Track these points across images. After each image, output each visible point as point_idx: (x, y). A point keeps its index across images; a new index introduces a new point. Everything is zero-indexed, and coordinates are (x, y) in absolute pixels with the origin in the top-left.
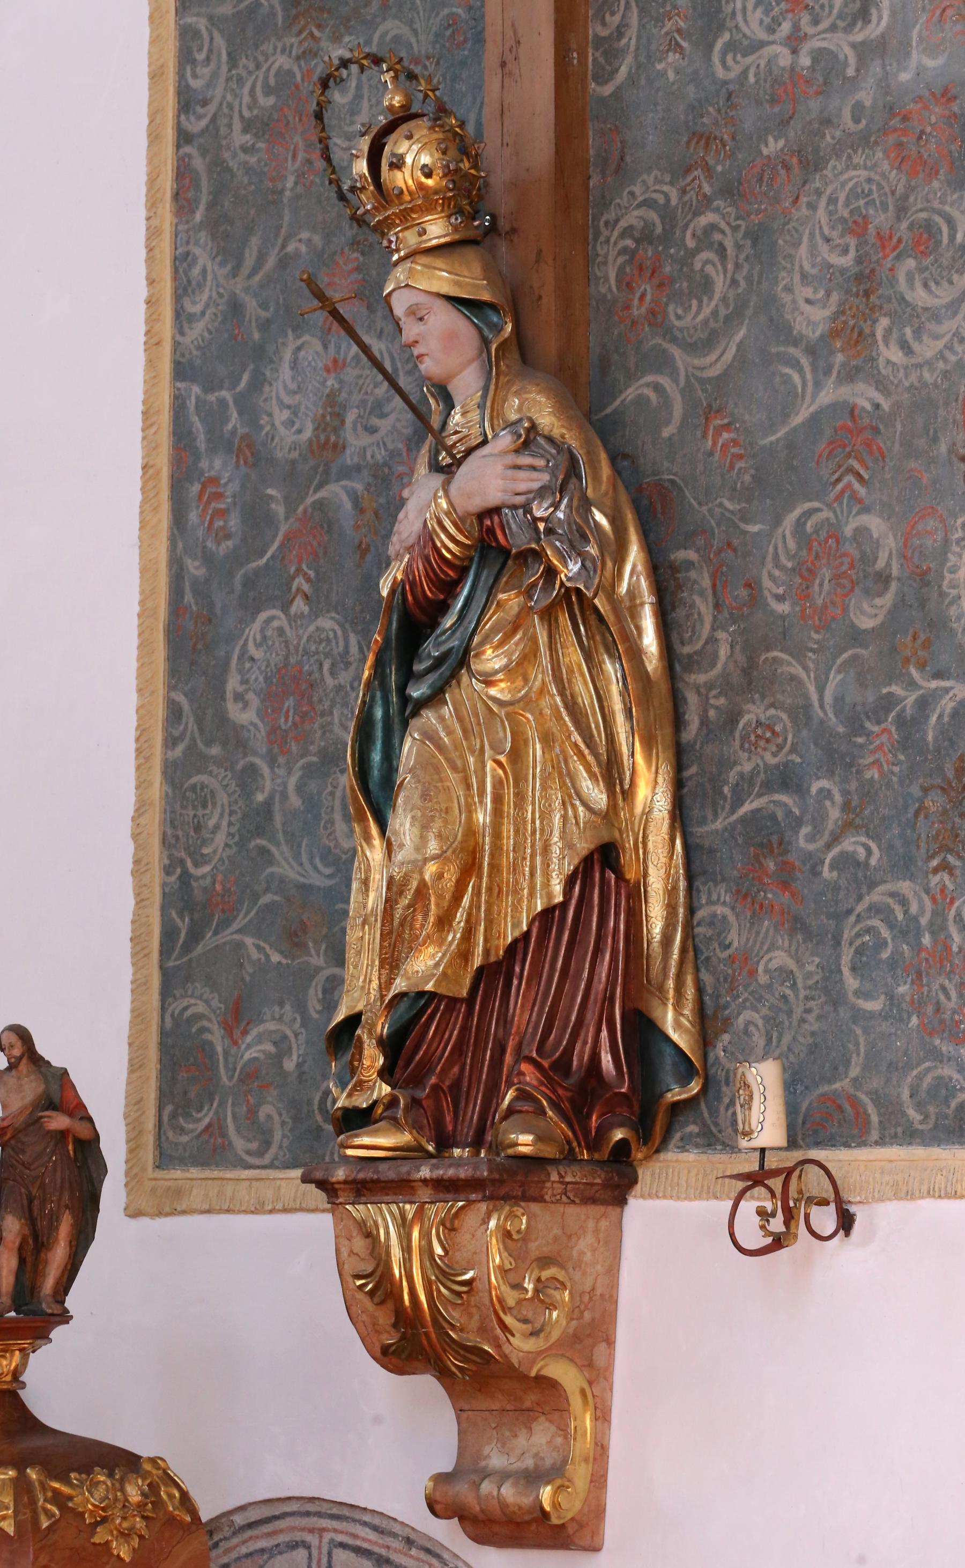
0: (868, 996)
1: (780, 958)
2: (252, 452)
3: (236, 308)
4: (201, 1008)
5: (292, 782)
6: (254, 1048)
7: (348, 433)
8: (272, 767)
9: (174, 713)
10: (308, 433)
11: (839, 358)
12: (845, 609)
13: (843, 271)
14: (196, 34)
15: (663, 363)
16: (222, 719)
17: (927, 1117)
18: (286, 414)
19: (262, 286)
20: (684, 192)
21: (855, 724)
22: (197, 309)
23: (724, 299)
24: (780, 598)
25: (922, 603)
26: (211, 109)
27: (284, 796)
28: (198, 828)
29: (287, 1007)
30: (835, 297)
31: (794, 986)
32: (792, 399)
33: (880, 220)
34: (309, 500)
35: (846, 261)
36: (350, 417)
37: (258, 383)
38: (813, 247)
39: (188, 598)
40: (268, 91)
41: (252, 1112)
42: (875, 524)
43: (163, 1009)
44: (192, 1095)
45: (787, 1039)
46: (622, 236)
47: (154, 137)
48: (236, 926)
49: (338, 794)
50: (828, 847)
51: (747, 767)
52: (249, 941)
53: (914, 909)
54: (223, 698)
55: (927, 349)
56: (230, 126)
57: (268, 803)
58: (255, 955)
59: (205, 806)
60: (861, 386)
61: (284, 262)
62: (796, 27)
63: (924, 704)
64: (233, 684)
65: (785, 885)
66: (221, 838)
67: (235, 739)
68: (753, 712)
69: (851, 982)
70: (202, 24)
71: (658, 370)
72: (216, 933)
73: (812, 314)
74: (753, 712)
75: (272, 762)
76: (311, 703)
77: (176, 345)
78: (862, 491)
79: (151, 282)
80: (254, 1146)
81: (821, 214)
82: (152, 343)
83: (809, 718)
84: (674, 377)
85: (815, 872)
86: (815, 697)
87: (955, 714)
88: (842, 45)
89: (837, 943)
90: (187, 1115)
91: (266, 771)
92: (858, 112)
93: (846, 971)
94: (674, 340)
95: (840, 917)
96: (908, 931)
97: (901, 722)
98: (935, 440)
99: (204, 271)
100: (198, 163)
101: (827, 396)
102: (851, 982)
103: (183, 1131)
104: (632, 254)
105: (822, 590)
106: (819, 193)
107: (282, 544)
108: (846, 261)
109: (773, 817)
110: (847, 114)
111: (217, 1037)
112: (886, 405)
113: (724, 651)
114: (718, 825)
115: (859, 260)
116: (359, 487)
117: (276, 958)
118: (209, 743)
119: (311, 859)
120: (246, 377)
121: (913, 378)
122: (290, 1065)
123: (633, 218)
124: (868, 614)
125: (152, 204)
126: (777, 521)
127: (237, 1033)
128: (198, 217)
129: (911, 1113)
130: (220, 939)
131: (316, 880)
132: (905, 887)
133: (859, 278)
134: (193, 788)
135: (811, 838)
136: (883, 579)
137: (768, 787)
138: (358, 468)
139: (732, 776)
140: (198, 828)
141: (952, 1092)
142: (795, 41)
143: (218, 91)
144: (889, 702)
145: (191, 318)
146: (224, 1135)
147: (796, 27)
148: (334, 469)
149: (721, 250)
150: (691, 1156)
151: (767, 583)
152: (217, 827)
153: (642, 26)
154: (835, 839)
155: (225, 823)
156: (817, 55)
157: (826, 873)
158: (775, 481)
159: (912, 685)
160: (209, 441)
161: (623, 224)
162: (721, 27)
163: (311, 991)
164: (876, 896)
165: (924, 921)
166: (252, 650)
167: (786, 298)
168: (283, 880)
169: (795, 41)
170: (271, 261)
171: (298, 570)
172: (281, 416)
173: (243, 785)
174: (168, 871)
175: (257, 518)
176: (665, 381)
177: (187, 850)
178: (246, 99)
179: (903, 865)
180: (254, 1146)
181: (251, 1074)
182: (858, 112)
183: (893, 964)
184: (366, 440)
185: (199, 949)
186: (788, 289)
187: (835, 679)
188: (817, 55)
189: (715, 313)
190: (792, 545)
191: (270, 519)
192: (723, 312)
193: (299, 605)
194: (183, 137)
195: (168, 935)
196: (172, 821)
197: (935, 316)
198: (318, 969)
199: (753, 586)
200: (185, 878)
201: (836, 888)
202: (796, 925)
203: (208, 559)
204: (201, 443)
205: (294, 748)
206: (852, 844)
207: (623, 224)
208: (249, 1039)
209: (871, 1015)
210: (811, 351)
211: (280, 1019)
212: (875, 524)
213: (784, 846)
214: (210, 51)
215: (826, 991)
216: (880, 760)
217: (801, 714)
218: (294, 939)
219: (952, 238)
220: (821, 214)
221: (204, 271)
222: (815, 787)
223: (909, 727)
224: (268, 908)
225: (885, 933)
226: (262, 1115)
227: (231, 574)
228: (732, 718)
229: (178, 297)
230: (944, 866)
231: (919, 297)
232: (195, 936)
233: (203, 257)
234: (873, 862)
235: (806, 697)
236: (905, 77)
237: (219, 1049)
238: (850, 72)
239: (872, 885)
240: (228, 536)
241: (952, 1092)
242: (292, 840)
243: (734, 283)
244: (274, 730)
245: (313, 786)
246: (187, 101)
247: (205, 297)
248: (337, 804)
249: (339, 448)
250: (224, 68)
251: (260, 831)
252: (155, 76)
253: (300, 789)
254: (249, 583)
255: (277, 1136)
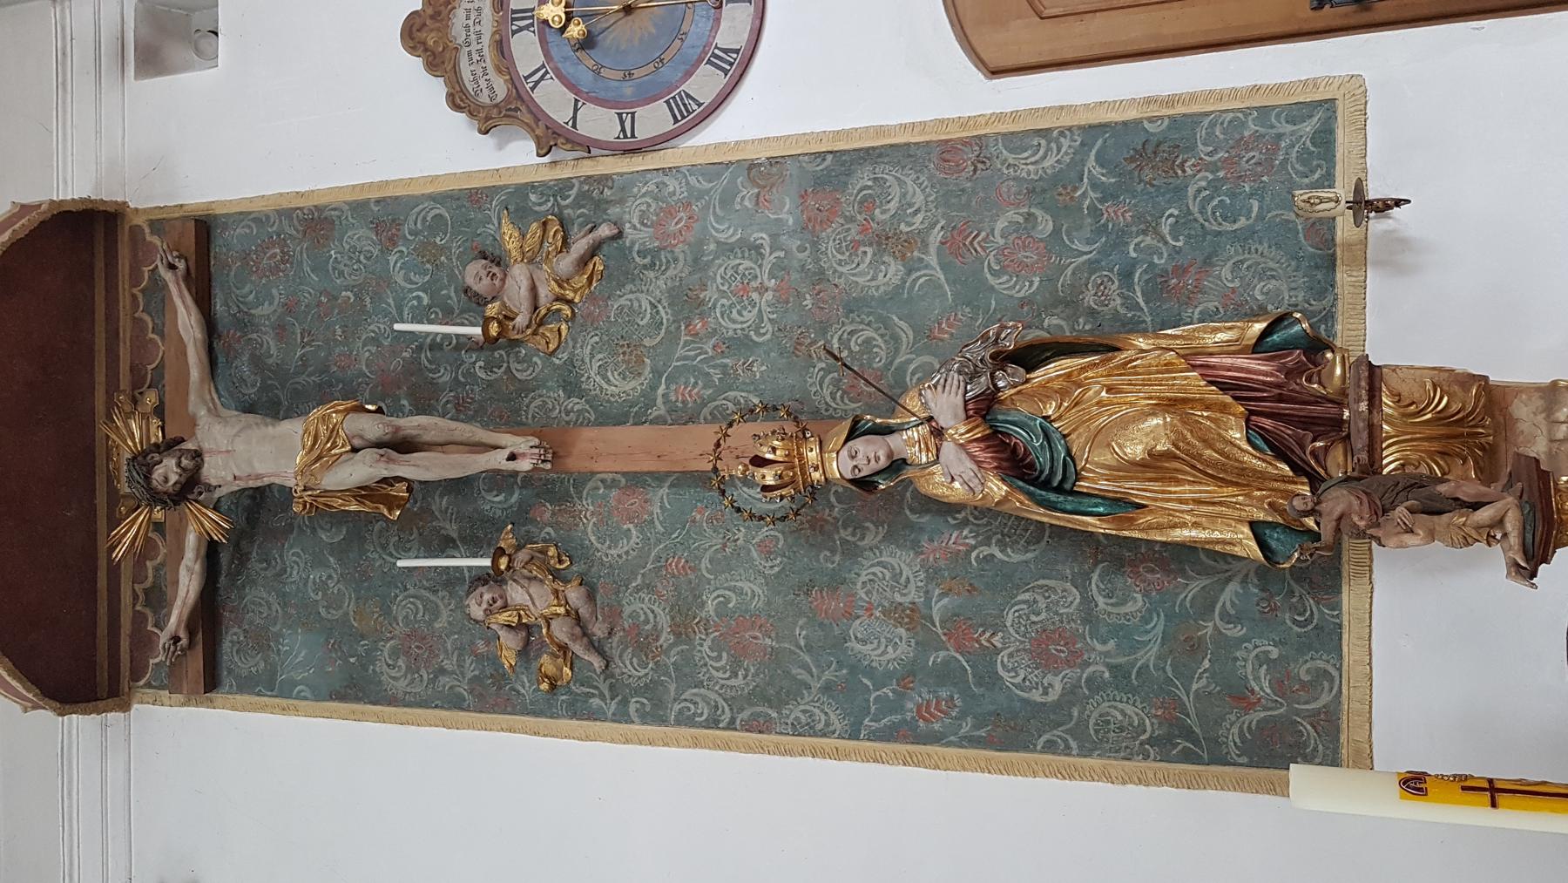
0: (1250, 211)
1: (1226, 272)
2: (908, 675)
3: (827, 688)
4: (1235, 730)
5: (1099, 647)
6: (1262, 685)
7: (906, 600)
8: (1089, 664)
9: (1050, 747)
10: (902, 631)
11: (916, 253)
12: (1041, 240)
13: (874, 255)
14: (681, 712)
15: (902, 369)
16: (1057, 705)
17: (1319, 166)
18: (890, 649)
19: (818, 667)
20: (820, 359)
21: (1101, 230)
22: (823, 718)
23: (876, 330)
24: (1031, 283)
25: (1044, 191)
26: (721, 702)
27: (1107, 654)
28: (1122, 729)
29: (1238, 654)
30: (886, 259)
31: (1242, 262)
32: (932, 283)
33: (854, 233)
34: (940, 631)
35: (869, 251)
36: (898, 598)
37: (870, 671)
38: (861, 274)
39: (982, 733)
40: (719, 658)
41: (1304, 686)
42: (1000, 225)
43: (1235, 764)
44: (1290, 739)
45: (1271, 264)
46: (834, 399)
47: (726, 746)
48: (1185, 698)
49: (1109, 609)
50: (1166, 243)
51: (1119, 301)
52: (1195, 687)
53: (1204, 184)
54: (1044, 704)
55: (919, 199)
56: (732, 687)
57: (1112, 668)
58: (1204, 682)
59: (1108, 722)
60: (931, 239)
61: (809, 649)
62: (756, 289)
63: (1095, 185)
64: (1036, 696)
65: (1186, 271)
66: (1129, 710)
67: (1070, 693)
68: (1089, 300)
69: (1242, 222)
70: (677, 707)
71: (905, 372)
72: (1188, 716)
73: (893, 271)
74: (1089, 300)
75: (1087, 664)
76: (1054, 632)
77: (840, 737)
78: (983, 234)
79: (803, 753)
80: (1326, 684)
81: (844, 269)
82: (837, 755)
83: (1098, 261)
84: (909, 362)
85: (1178, 251)
86: (1086, 257)
87: (1102, 166)
88: (770, 259)
89: (1219, 233)
90: (1306, 745)
91: (1091, 669)
92: (802, 249)
93: (1236, 227)
94: (891, 363)
95: (1205, 232)
96: (1215, 186)
97: (1102, 200)
98: (963, 190)
99: (804, 712)
100: (745, 715)
101: (932, 259)
102: (1242, 222)
103: (1315, 749)
104: (844, 392)
105: (1030, 256)
106: (835, 271)
107: (962, 654)
108: (869, 251)
109: (1147, 282)
110: (801, 256)
111: (1257, 716)
112: (943, 222)
113: (1055, 321)
114: (1148, 319)
115: (871, 245)
116: (937, 592)
117: (1206, 664)
118: (1071, 716)
119: (1147, 632)
120: (865, 681)
121: (931, 206)
122: (1275, 653)
123: (826, 393)
124: (1045, 225)
125: (762, 749)
126: (992, 288)
127: (1253, 699)
128: (774, 715)
129: (1317, 176)
130: (1192, 712)
131: (1160, 628)
132: (1191, 191)
133: (879, 244)
134: (1096, 732)
135: (1160, 255)
136: (1029, 217)
137: (1130, 287)
138: (927, 592)
139: (1122, 311)
140: (1122, 729)
141: (1305, 149)
142: (762, 290)
143: (713, 696)
144: (1093, 210)
145: (827, 724)
146: (1318, 712)
147: (756, 289)
148: (924, 611)
149: (852, 333)
150: (1339, 327)
151: (1021, 294)
152: (1123, 712)
153: (737, 389)
154: (1163, 239)
155: (1120, 705)
156: (772, 276)
157: (1180, 244)
158: (972, 290)
159: (1084, 195)
160: (897, 713)
161: (828, 399)
162: (747, 336)
163: (1229, 633)
164: (1195, 210)
165: (1211, 177)
166: (1018, 680)
167: (882, 289)
168: (1159, 658)
169: (762, 290)
170: (808, 659)
171: (978, 641)
172: (891, 653)
173: (1099, 689)
174: (1146, 757)
175: (946, 674)
176: (912, 367)
177: (1135, 739)
178: (720, 675)
179: (1179, 192)
180: (1326, 684)
181: (1279, 686)
182: (802, 249)
183: (1233, 196)
184: (912, 587)
185: (1197, 730)
186: (878, 288)
187: (1077, 246)
188: (772, 276)
189: (882, 336)
190: (1005, 278)
191: (946, 662)
192: (882, 331)
193: (997, 641)
194: (731, 726)
195: (1188, 757)
196: (1116, 752)
197: (904, 195)
198: (1216, 627)
199: (1023, 302)
200: (1152, 741)
201: (1189, 236)
202: (1208, 262)
203: (963, 715)
204: (896, 718)
205: (1079, 645)
206: (1165, 230)
207: (828, 399)
208: (1257, 689)
209: (1260, 208)
210: (909, 273)
211: (1245, 660)
212: (1000, 225)
213: (1164, 273)
214: (691, 701)
215: (1246, 239)
216: (1119, 214)
217: (1093, 267)
218: (1195, 648)
219: (869, 187)
220: (844, 269)
221: (804, 712)
222: (1133, 255)
223: (1108, 195)
224: (1175, 668)
225: (1215, 202)
226: (1306, 678)
227: (973, 696)
228: (1092, 313)
229: (815, 735)
230: (1182, 166)
231: (893, 206)
232: (1189, 734)
233: (795, 712)
234: (1176, 213)
235: (1084, 263)
236: (791, 222)
237: (1262, 715)
238: (782, 254)
239: (1189, 213)
240: (952, 698)
241: (1305, 149)
242: (1135, 647)
243: (869, 324)
244: (1068, 663)
245: (1103, 630)
246: (713, 723)
247: (817, 711)
248: (1115, 610)
249: (914, 607)
250: (702, 691)
251: (1127, 676)
252: (696, 743)
253: (1104, 642)
254: (979, 684)
255: (1320, 664)
